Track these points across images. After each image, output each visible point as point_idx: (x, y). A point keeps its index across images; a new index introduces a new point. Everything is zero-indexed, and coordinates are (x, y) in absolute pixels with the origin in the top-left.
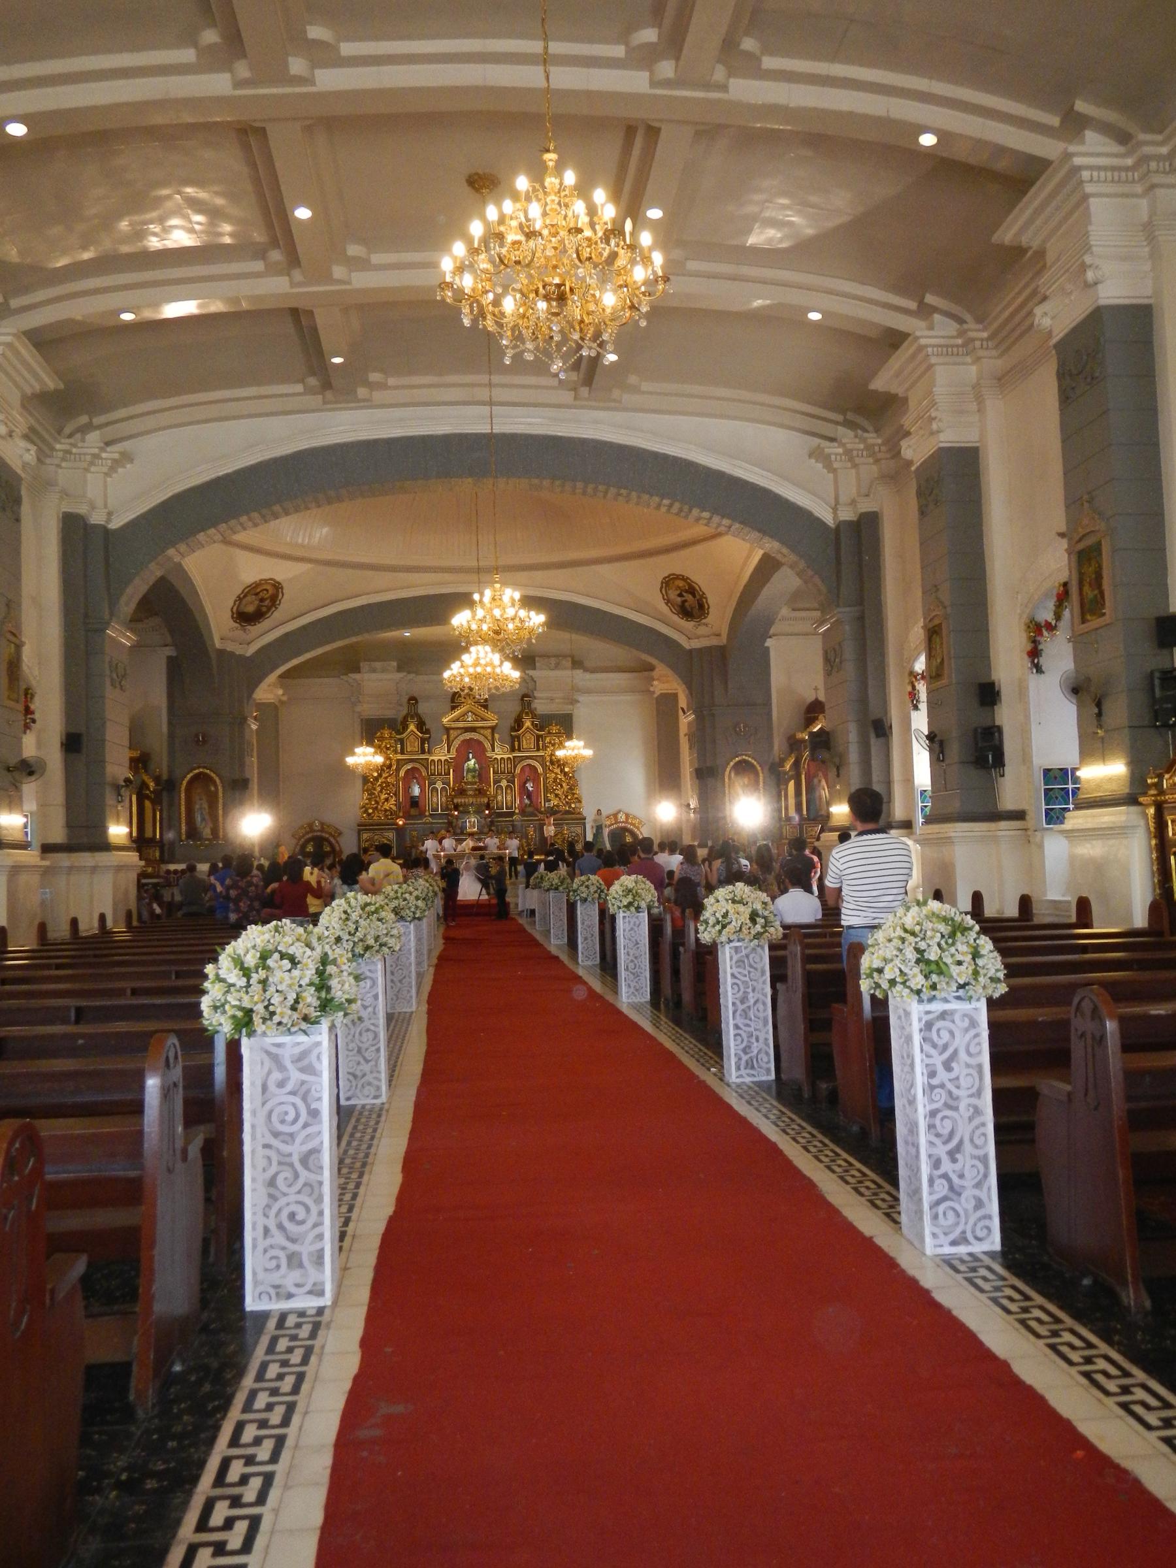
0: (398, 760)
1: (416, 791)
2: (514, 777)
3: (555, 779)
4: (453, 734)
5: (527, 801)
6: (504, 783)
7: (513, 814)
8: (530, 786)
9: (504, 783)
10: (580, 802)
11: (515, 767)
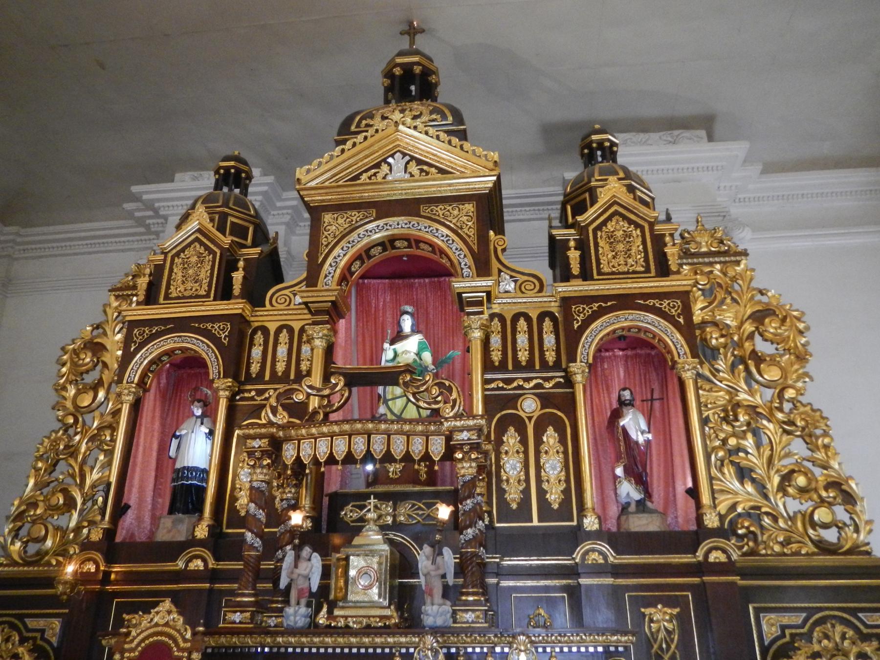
0: (133, 325)
1: (198, 449)
2: (569, 382)
3: (729, 413)
4: (332, 223)
5: (628, 490)
6: (530, 406)
7: (577, 535)
8: (634, 424)
9: (530, 406)
10: (849, 499)
11: (570, 341)
